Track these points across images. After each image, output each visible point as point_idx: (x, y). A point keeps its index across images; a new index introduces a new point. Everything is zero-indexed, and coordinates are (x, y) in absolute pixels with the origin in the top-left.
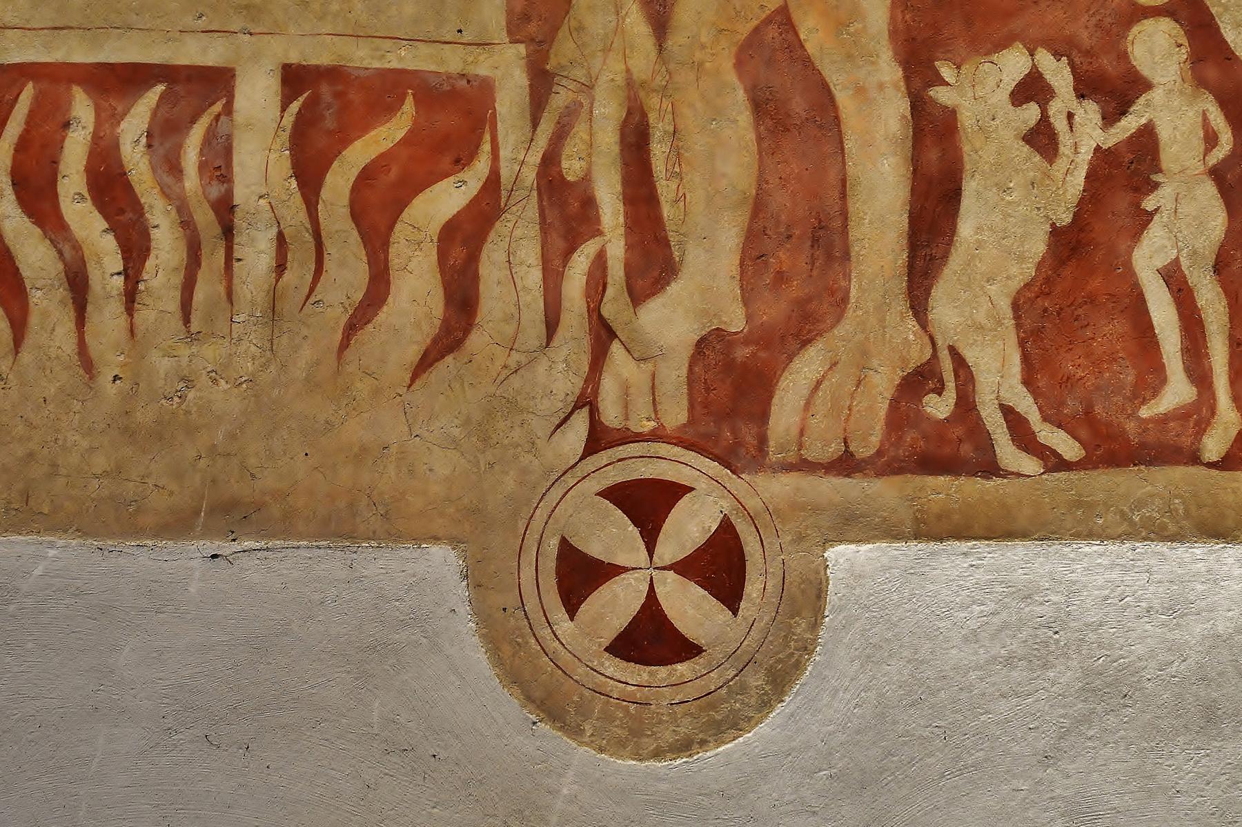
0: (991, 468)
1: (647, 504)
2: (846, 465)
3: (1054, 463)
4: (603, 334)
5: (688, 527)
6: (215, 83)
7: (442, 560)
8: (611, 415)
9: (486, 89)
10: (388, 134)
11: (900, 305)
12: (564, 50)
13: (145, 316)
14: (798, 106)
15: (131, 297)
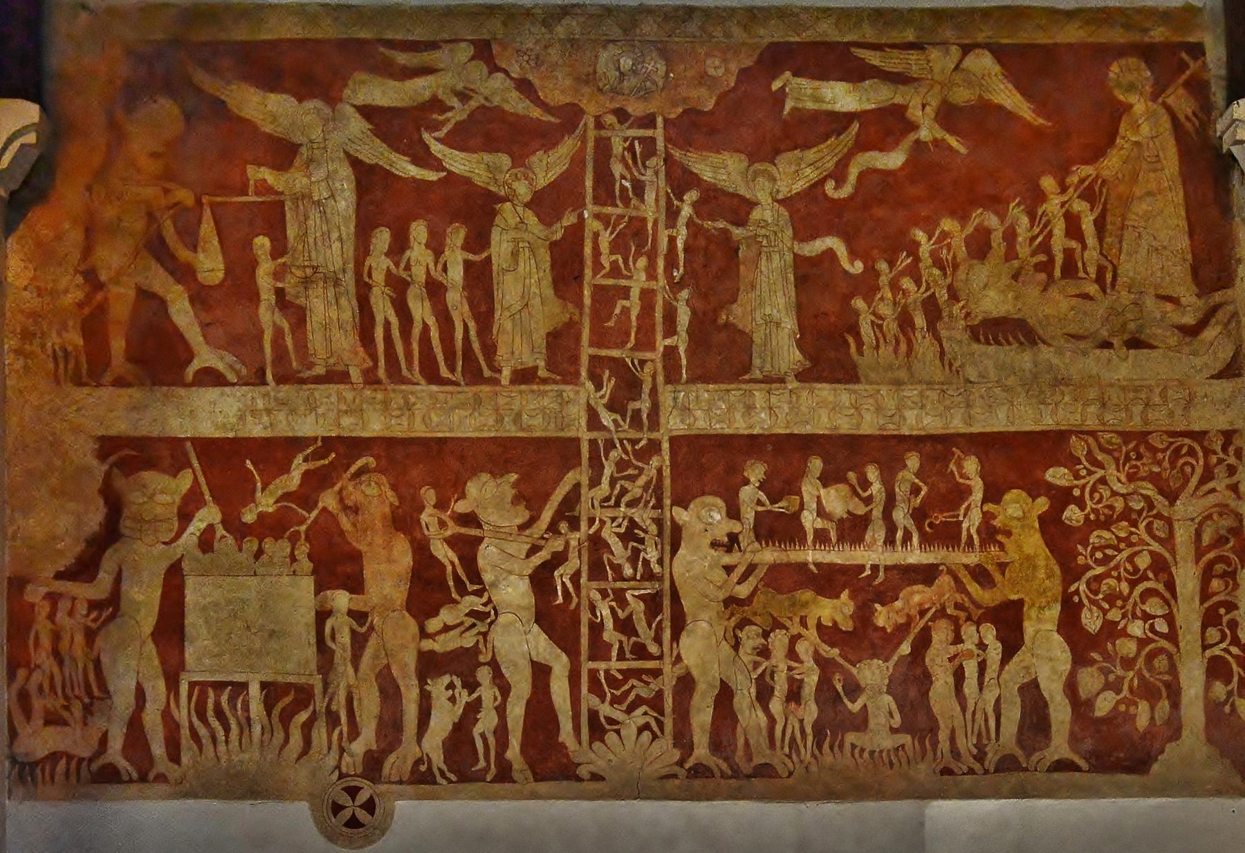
0: (435, 783)
1: (353, 792)
2: (401, 782)
3: (450, 782)
4: (342, 750)
5: (363, 797)
6: (244, 686)
7: (304, 806)
8: (344, 770)
9: (312, 686)
10: (287, 700)
11: (414, 743)
12: (332, 676)
13: (230, 746)
14: (391, 691)
15: (227, 742)
